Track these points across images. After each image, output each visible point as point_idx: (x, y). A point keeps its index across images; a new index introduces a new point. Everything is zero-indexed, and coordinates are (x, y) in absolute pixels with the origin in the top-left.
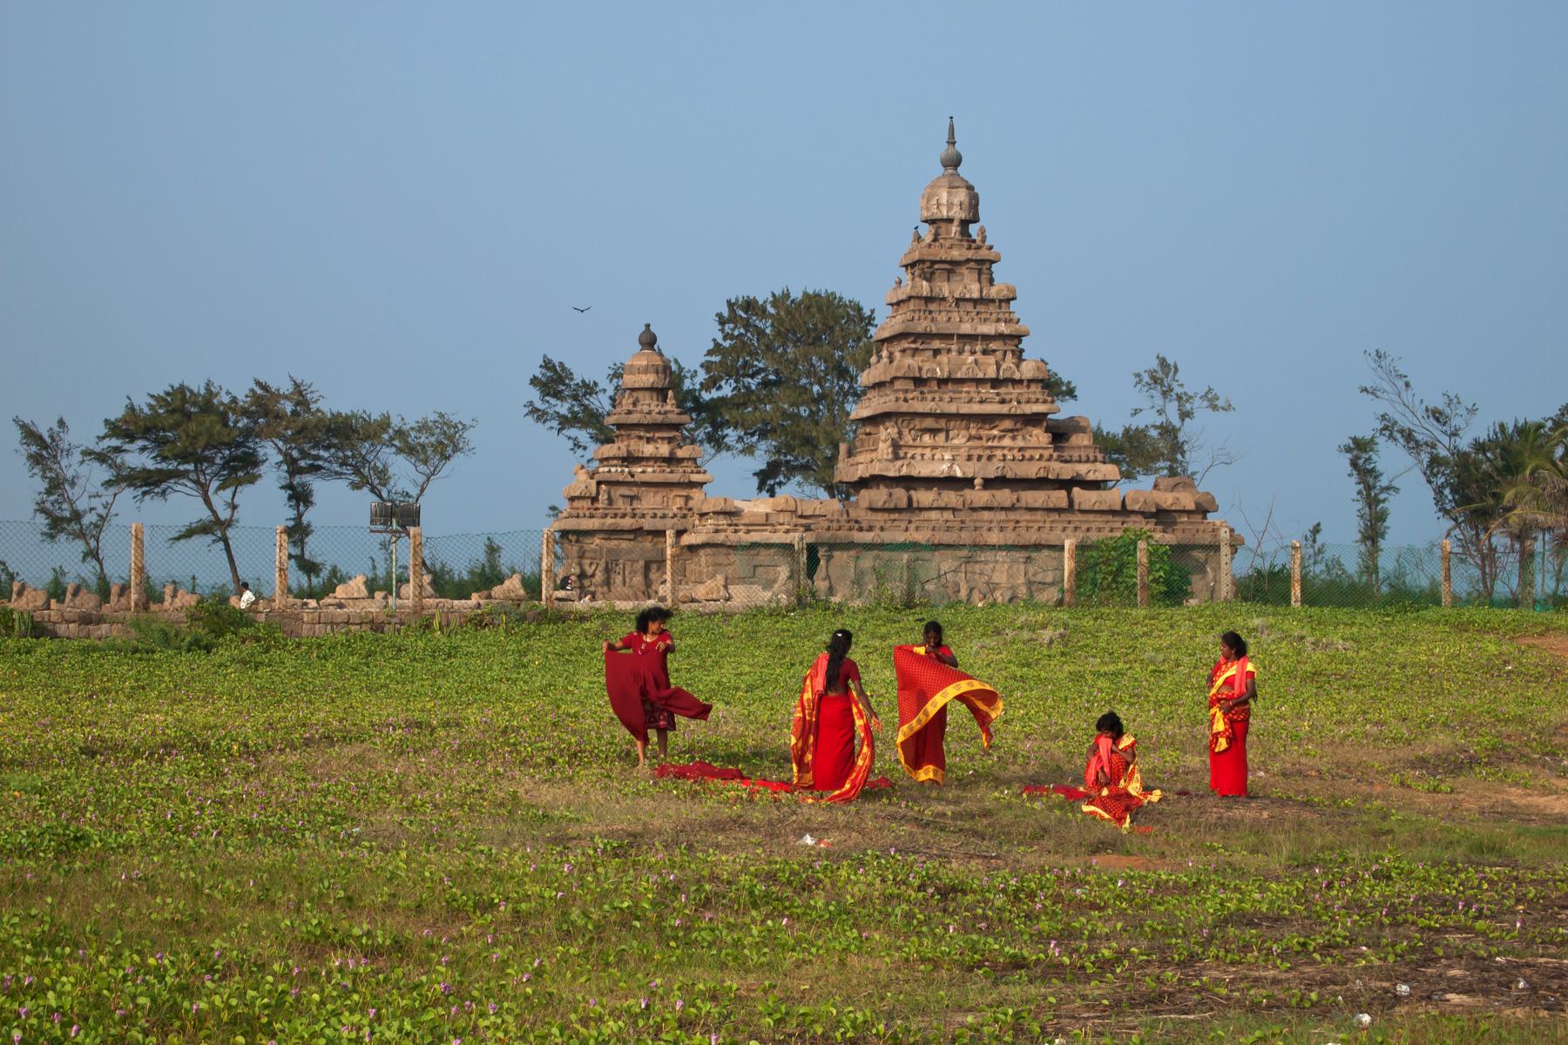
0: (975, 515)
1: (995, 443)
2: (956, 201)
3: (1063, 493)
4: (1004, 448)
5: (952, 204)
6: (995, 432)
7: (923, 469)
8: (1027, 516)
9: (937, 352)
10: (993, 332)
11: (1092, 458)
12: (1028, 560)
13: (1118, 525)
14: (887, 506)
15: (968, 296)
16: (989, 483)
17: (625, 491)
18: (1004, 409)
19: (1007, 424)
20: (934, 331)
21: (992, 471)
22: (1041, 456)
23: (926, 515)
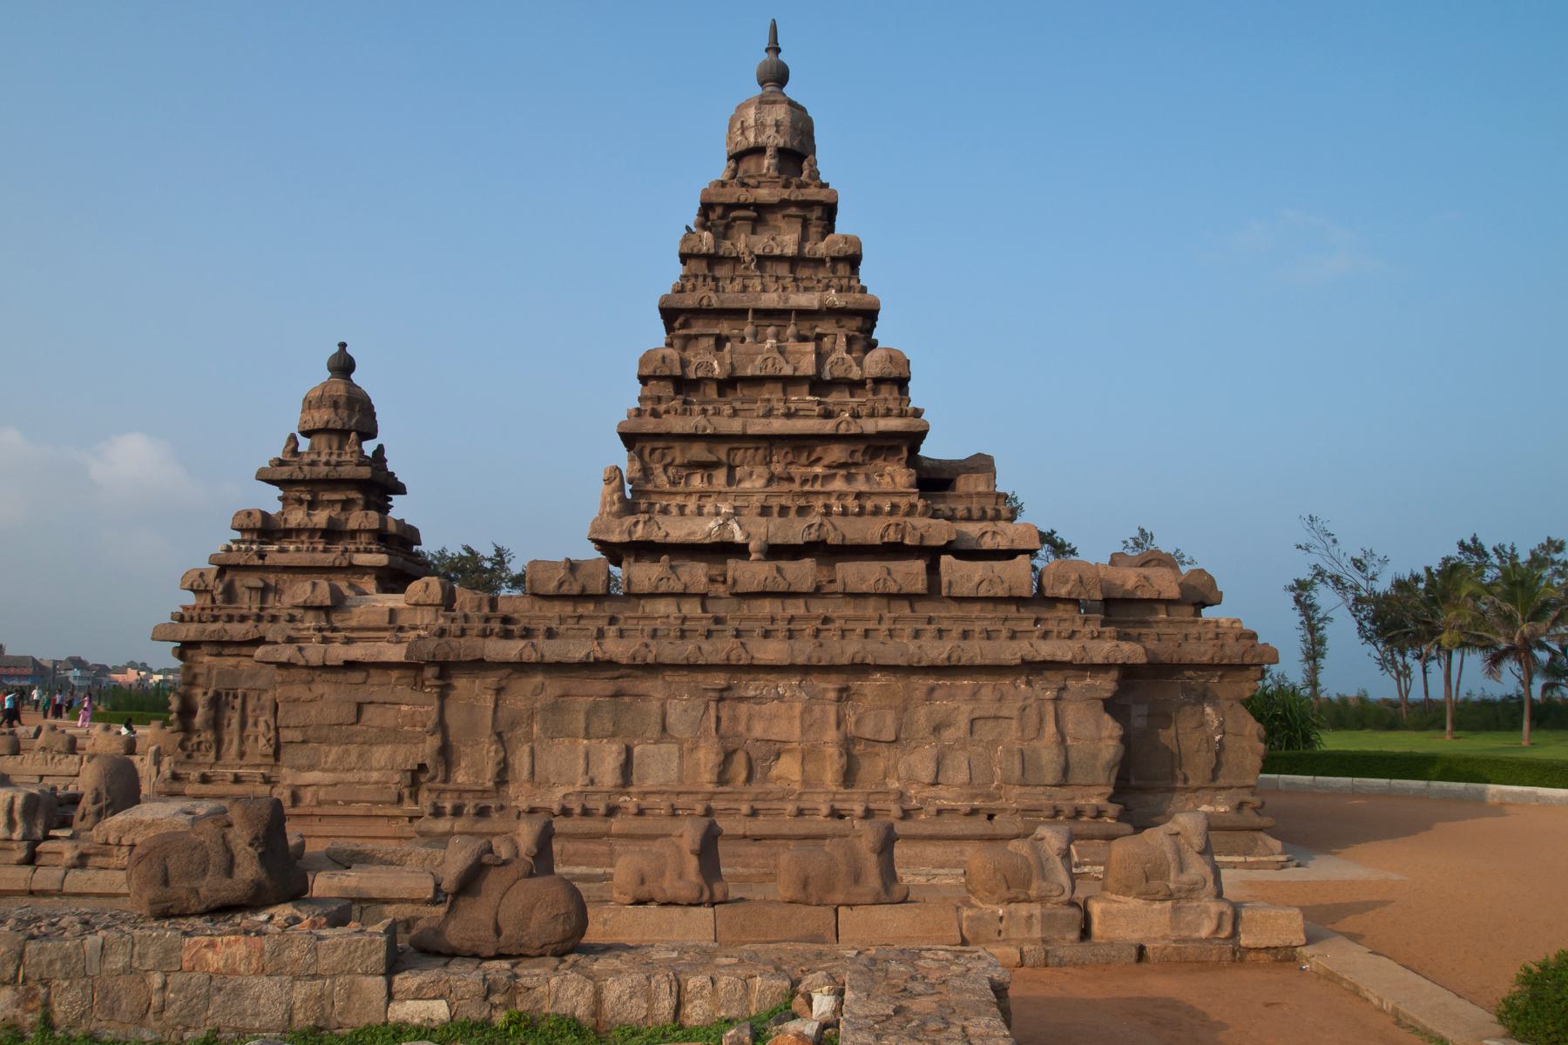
0: (747, 608)
1: (817, 487)
2: (770, 120)
3: (919, 566)
4: (829, 494)
5: (763, 125)
6: (818, 470)
7: (676, 530)
8: (848, 609)
9: (720, 341)
10: (816, 305)
11: (990, 513)
12: (844, 693)
13: (1027, 625)
14: (565, 589)
15: (777, 252)
16: (775, 552)
17: (254, 581)
18: (828, 427)
19: (837, 453)
20: (715, 303)
21: (796, 531)
22: (894, 507)
23: (650, 607)
